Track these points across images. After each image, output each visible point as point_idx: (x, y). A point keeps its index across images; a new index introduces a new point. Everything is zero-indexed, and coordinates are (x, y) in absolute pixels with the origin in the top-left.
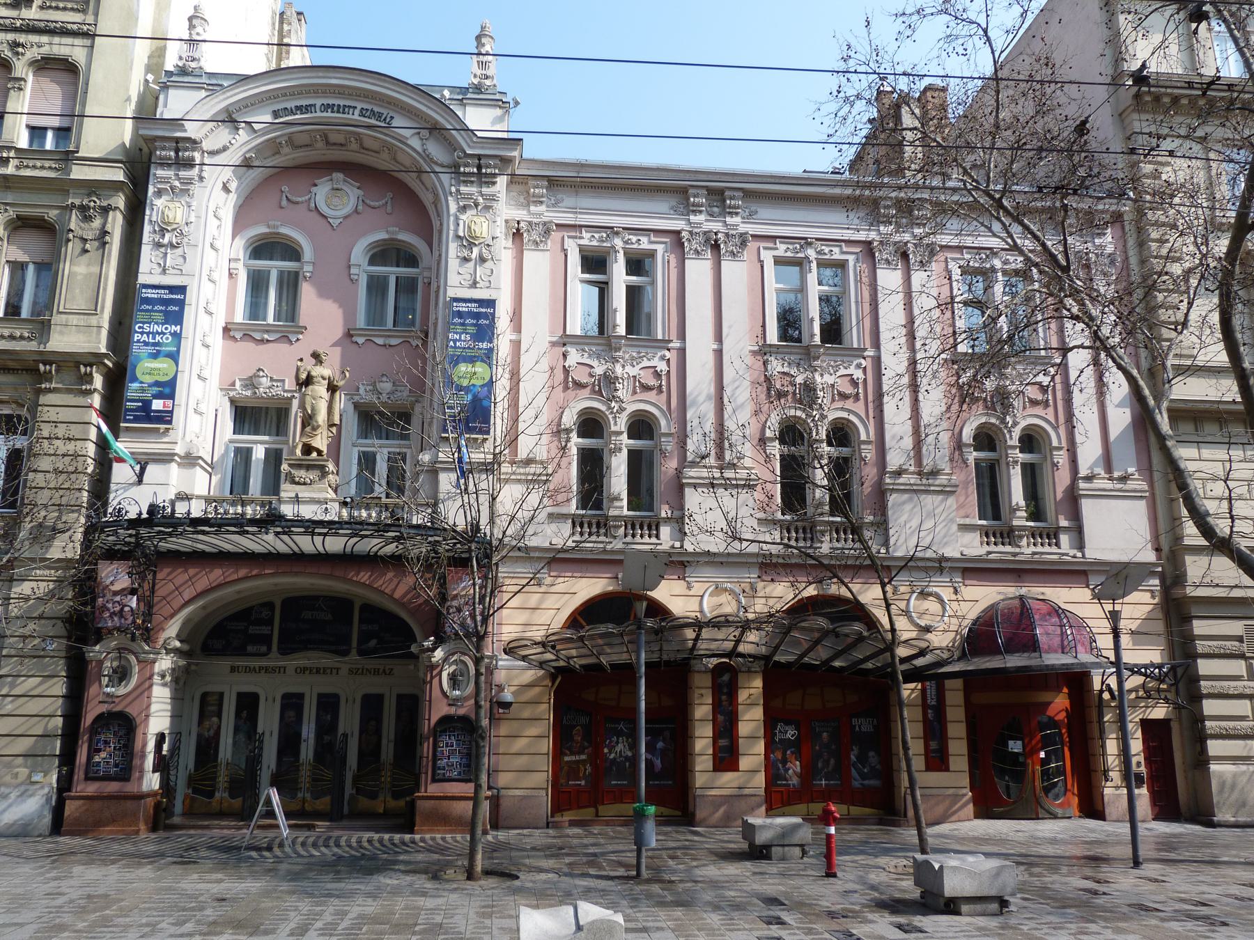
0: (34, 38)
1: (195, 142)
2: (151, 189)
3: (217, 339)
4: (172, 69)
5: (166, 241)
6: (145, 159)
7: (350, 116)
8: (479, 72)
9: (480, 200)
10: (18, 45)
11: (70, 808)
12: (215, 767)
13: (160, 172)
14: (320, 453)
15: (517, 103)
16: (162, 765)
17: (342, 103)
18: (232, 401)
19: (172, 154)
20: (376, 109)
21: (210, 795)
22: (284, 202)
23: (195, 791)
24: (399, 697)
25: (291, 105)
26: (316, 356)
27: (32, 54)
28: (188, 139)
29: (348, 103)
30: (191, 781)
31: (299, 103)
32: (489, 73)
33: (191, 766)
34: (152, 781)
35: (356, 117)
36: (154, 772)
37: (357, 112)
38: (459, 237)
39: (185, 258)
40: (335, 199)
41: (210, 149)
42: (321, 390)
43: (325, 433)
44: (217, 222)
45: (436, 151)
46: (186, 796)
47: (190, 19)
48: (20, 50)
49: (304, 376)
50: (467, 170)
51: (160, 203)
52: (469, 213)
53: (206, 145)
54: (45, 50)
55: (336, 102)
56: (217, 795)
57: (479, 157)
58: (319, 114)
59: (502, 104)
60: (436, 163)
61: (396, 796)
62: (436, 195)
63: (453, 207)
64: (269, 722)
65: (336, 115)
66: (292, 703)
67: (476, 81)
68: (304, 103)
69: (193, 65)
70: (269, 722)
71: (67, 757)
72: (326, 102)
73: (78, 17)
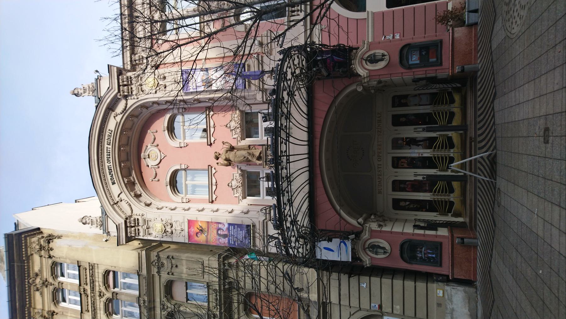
0: (97, 289)
1: (127, 219)
2: (149, 238)
3: (214, 206)
4: (102, 231)
5: (170, 230)
6: (143, 242)
7: (111, 149)
8: (88, 92)
9: (138, 84)
10: (100, 295)
11: (459, 275)
12: (435, 201)
13: (141, 234)
14: (260, 153)
15: (97, 71)
16: (433, 226)
17: (106, 154)
18: (244, 198)
19: (133, 229)
20: (107, 138)
21: (452, 204)
22: (156, 179)
23: (449, 211)
24: (393, 106)
25: (109, 177)
26: (217, 158)
27: (103, 289)
28: (126, 222)
29: (105, 151)
30: (445, 214)
31: (108, 173)
32: (88, 88)
33: (435, 214)
34: (443, 232)
35: (111, 147)
36: (436, 230)
37: (109, 146)
38: (156, 92)
39: (177, 221)
40: (151, 155)
41: (130, 212)
42: (231, 155)
43: (252, 151)
44: (165, 208)
45: (120, 108)
46: (452, 216)
47: (84, 224)
48: (102, 294)
49: (226, 162)
50: (126, 91)
51: (154, 233)
52: (144, 87)
53: (129, 213)
54: (101, 284)
55: (106, 156)
56: (452, 200)
57: (119, 86)
58: (111, 164)
59: (98, 79)
60: (126, 107)
61: (452, 101)
62: (144, 106)
63: (142, 96)
64: (409, 174)
65: (111, 156)
66: (397, 163)
67: (91, 93)
68: (107, 171)
69: (99, 221)
70: (409, 174)
71: (428, 277)
72: (106, 161)
73: (88, 271)
